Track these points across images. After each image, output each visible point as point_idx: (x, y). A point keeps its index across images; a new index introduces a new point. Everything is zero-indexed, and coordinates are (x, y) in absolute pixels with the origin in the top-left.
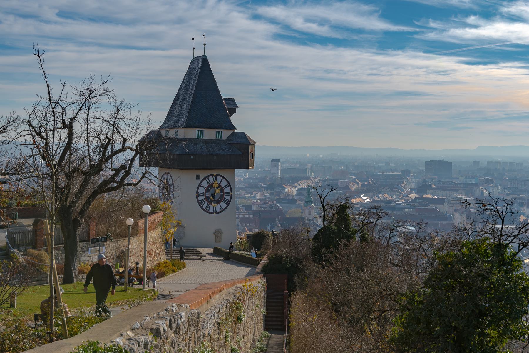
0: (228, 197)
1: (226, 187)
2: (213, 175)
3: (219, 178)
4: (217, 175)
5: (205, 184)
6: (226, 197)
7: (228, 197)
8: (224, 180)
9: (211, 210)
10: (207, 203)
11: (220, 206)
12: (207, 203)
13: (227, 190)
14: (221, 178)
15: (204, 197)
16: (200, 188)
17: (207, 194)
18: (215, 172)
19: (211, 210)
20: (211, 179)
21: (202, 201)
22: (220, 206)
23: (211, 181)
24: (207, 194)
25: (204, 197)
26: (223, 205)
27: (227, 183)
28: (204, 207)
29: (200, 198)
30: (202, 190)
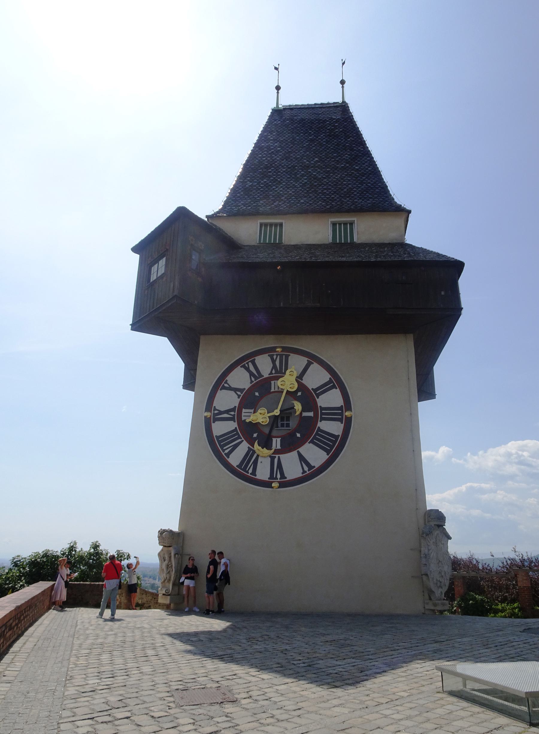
0: (334, 428)
2: (273, 349)
3: (297, 363)
4: (284, 349)
5: (240, 379)
8: (315, 366)
9: (263, 472)
10: (244, 446)
11: (302, 458)
12: (244, 446)
13: (331, 399)
14: (304, 361)
15: (232, 425)
19: (263, 472)
20: (265, 365)
22: (302, 458)
25: (232, 425)
26: (315, 455)
27: (326, 377)
28: (235, 459)
29: (220, 428)
30: (227, 400)
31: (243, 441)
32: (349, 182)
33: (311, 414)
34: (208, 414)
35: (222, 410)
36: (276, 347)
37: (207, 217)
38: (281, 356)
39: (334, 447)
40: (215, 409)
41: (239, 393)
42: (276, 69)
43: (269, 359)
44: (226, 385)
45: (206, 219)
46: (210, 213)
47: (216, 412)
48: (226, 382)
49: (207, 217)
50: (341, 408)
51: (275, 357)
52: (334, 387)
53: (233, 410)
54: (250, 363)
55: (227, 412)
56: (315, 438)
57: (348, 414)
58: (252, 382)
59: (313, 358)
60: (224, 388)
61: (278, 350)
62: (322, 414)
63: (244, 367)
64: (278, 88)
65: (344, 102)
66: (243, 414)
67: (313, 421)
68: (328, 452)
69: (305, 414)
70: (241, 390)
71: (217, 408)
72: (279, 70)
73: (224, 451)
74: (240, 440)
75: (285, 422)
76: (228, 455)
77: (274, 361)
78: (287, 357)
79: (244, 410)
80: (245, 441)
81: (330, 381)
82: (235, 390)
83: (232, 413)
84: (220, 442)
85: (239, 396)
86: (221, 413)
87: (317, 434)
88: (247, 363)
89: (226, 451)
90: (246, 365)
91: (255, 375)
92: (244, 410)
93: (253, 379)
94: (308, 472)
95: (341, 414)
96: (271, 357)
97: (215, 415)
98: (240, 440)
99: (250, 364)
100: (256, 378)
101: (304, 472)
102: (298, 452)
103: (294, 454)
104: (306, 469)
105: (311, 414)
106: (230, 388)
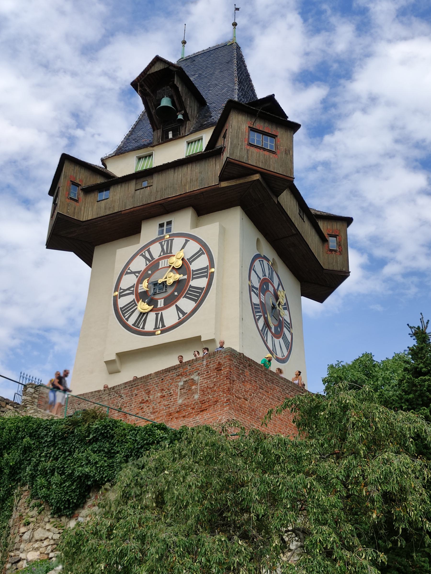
16: (253, 272)
23: (267, 275)
38: (271, 268)
50: (289, 324)
55: (256, 289)
60: (253, 270)
63: (259, 261)
70: (260, 279)
74: (260, 314)
78: (273, 271)
80: (263, 317)
89: (257, 317)
91: (264, 271)
96: (268, 265)
98: (260, 314)
106: (255, 272)
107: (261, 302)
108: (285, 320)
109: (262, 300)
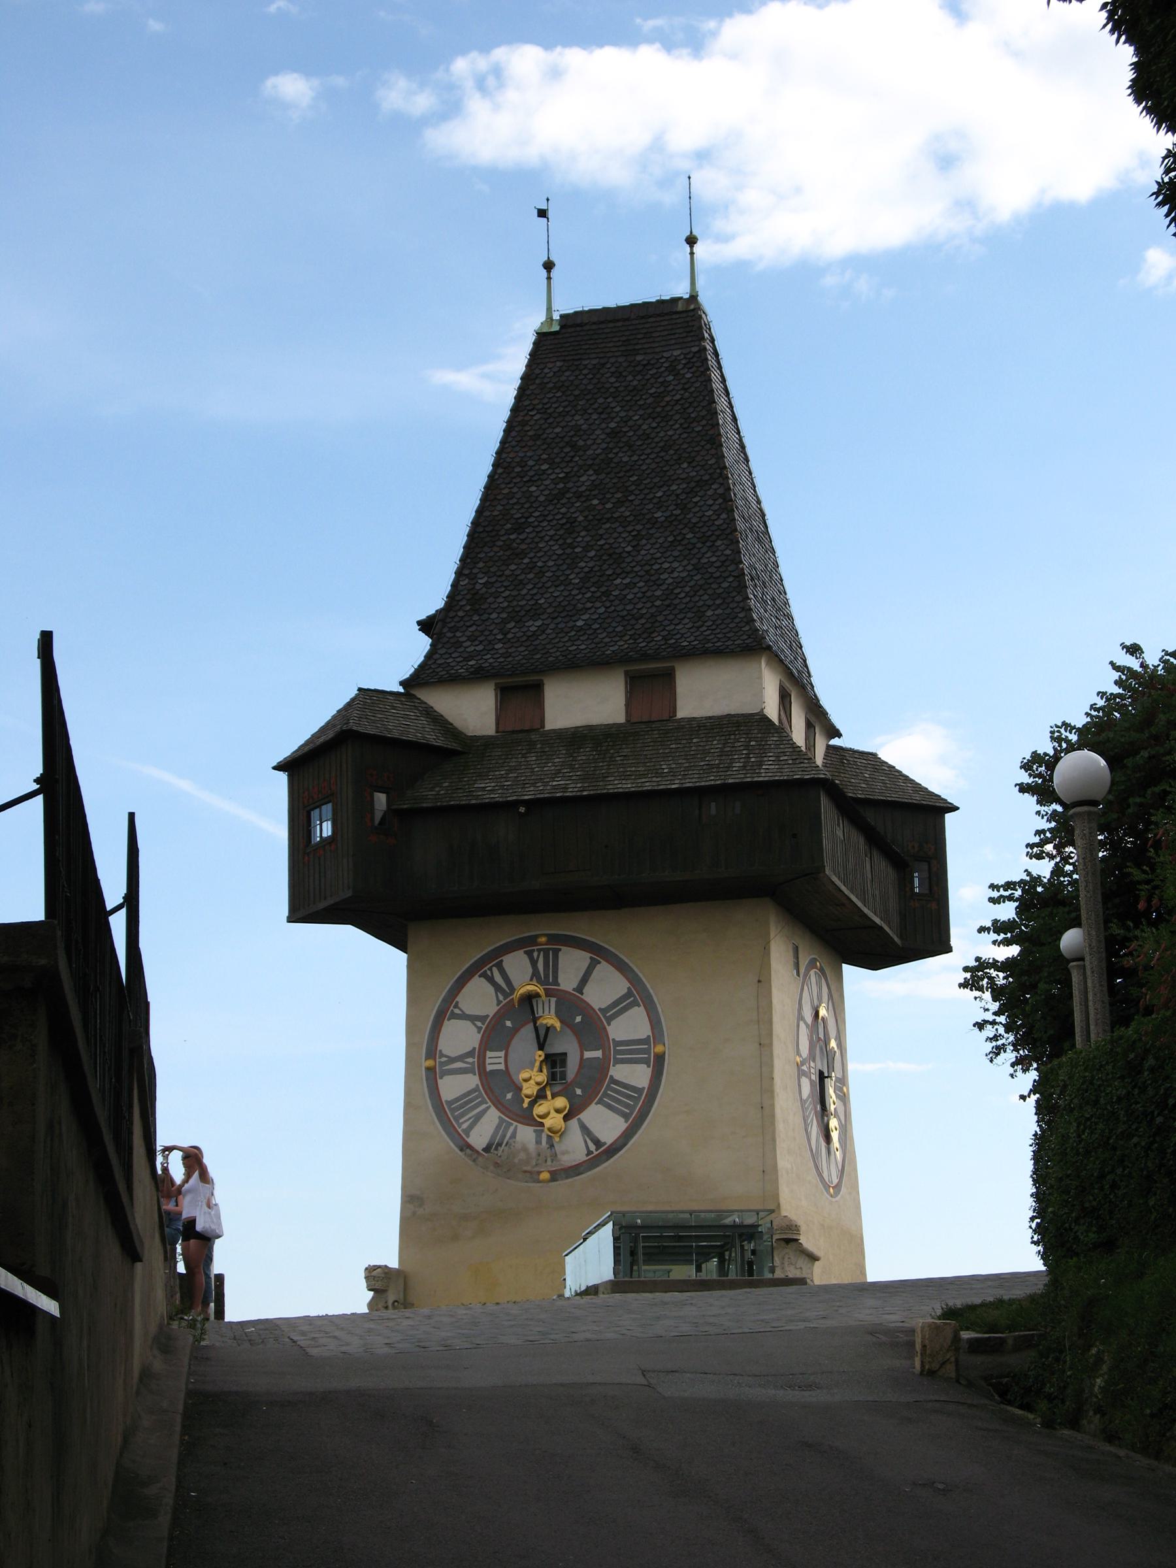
0: (637, 1075)
1: (620, 1006)
2: (532, 941)
4: (553, 939)
5: (479, 998)
6: (619, 1072)
7: (637, 1075)
8: (604, 969)
10: (493, 1116)
11: (585, 1129)
17: (495, 1060)
18: (542, 927)
21: (465, 1101)
22: (585, 1129)
24: (495, 1060)
29: (453, 1087)
31: (488, 1108)
32: (676, 564)
33: (598, 1054)
34: (430, 1063)
35: (453, 1055)
36: (537, 936)
37: (402, 683)
38: (546, 952)
39: (639, 1108)
40: (442, 1055)
41: (479, 1024)
42: (542, 213)
43: (526, 959)
44: (457, 1011)
45: (401, 690)
46: (407, 672)
47: (444, 1059)
48: (456, 1006)
49: (402, 683)
50: (645, 1041)
51: (535, 954)
52: (635, 1004)
53: (470, 1054)
54: (494, 969)
55: (460, 1058)
56: (605, 1095)
57: (659, 1049)
58: (499, 1002)
59: (598, 952)
61: (543, 939)
62: (617, 1052)
63: (484, 975)
64: (549, 266)
65: (694, 298)
66: (488, 1061)
67: (602, 1067)
68: (626, 1116)
69: (588, 1055)
70: (482, 1019)
71: (444, 1052)
72: (550, 214)
73: (460, 1125)
74: (484, 1106)
75: (558, 1070)
76: (468, 1134)
77: (534, 963)
78: (556, 952)
79: (489, 1054)
80: (493, 1109)
81: (629, 994)
82: (472, 1019)
83: (470, 1060)
84: (453, 1110)
85: (479, 1029)
86: (453, 1060)
87: (608, 1087)
88: (490, 969)
89: (465, 1126)
90: (489, 973)
91: (505, 989)
92: (489, 1054)
93: (501, 997)
94: (596, 1153)
95: (647, 1051)
96: (529, 954)
97: (442, 1064)
98: (484, 1106)
99: (494, 969)
100: (506, 995)
101: (589, 1152)
102: (579, 1120)
103: (574, 1123)
104: (592, 1147)
105: (598, 1054)
106: (464, 1017)
107: (484, 1074)
108: (618, 1043)
109: (489, 1068)
